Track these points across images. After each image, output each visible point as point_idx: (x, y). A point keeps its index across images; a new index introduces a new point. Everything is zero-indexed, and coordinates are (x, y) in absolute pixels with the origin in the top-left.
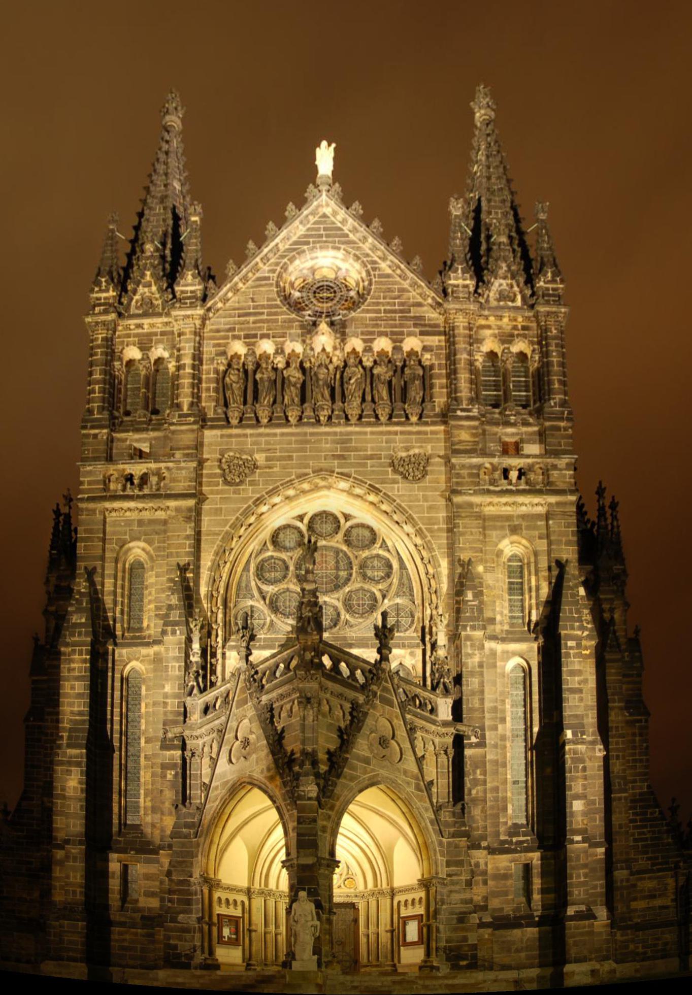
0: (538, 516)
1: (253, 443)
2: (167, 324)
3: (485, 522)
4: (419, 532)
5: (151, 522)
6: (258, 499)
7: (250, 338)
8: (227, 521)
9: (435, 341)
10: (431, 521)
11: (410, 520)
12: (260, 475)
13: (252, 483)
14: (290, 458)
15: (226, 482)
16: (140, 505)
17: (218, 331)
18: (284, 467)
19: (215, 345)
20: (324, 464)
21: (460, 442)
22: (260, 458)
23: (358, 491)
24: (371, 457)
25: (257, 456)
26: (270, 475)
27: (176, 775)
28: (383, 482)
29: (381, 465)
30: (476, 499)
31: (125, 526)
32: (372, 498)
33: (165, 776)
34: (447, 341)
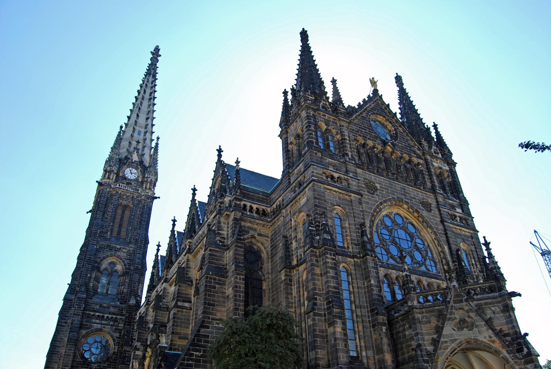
0: (467, 236)
1: (375, 179)
2: (335, 120)
3: (457, 235)
4: (435, 233)
5: (344, 199)
6: (381, 203)
7: (364, 137)
8: (372, 208)
9: (421, 161)
10: (438, 229)
11: (431, 227)
12: (380, 193)
13: (377, 195)
14: (388, 189)
15: (368, 192)
16: (340, 191)
17: (353, 130)
18: (387, 192)
19: (353, 135)
20: (399, 196)
21: (440, 202)
22: (378, 186)
23: (411, 210)
24: (414, 198)
25: (377, 185)
26: (383, 194)
27: (386, 329)
28: (420, 209)
29: (417, 202)
30: (451, 225)
31: (333, 197)
32: (416, 214)
33: (382, 330)
34: (426, 162)
